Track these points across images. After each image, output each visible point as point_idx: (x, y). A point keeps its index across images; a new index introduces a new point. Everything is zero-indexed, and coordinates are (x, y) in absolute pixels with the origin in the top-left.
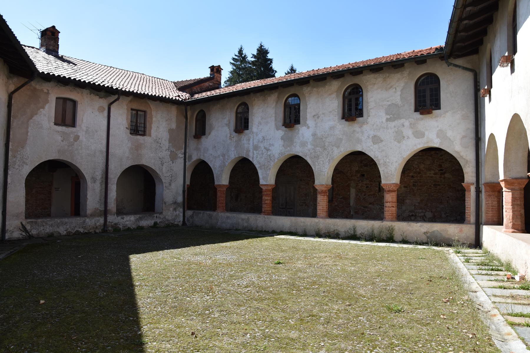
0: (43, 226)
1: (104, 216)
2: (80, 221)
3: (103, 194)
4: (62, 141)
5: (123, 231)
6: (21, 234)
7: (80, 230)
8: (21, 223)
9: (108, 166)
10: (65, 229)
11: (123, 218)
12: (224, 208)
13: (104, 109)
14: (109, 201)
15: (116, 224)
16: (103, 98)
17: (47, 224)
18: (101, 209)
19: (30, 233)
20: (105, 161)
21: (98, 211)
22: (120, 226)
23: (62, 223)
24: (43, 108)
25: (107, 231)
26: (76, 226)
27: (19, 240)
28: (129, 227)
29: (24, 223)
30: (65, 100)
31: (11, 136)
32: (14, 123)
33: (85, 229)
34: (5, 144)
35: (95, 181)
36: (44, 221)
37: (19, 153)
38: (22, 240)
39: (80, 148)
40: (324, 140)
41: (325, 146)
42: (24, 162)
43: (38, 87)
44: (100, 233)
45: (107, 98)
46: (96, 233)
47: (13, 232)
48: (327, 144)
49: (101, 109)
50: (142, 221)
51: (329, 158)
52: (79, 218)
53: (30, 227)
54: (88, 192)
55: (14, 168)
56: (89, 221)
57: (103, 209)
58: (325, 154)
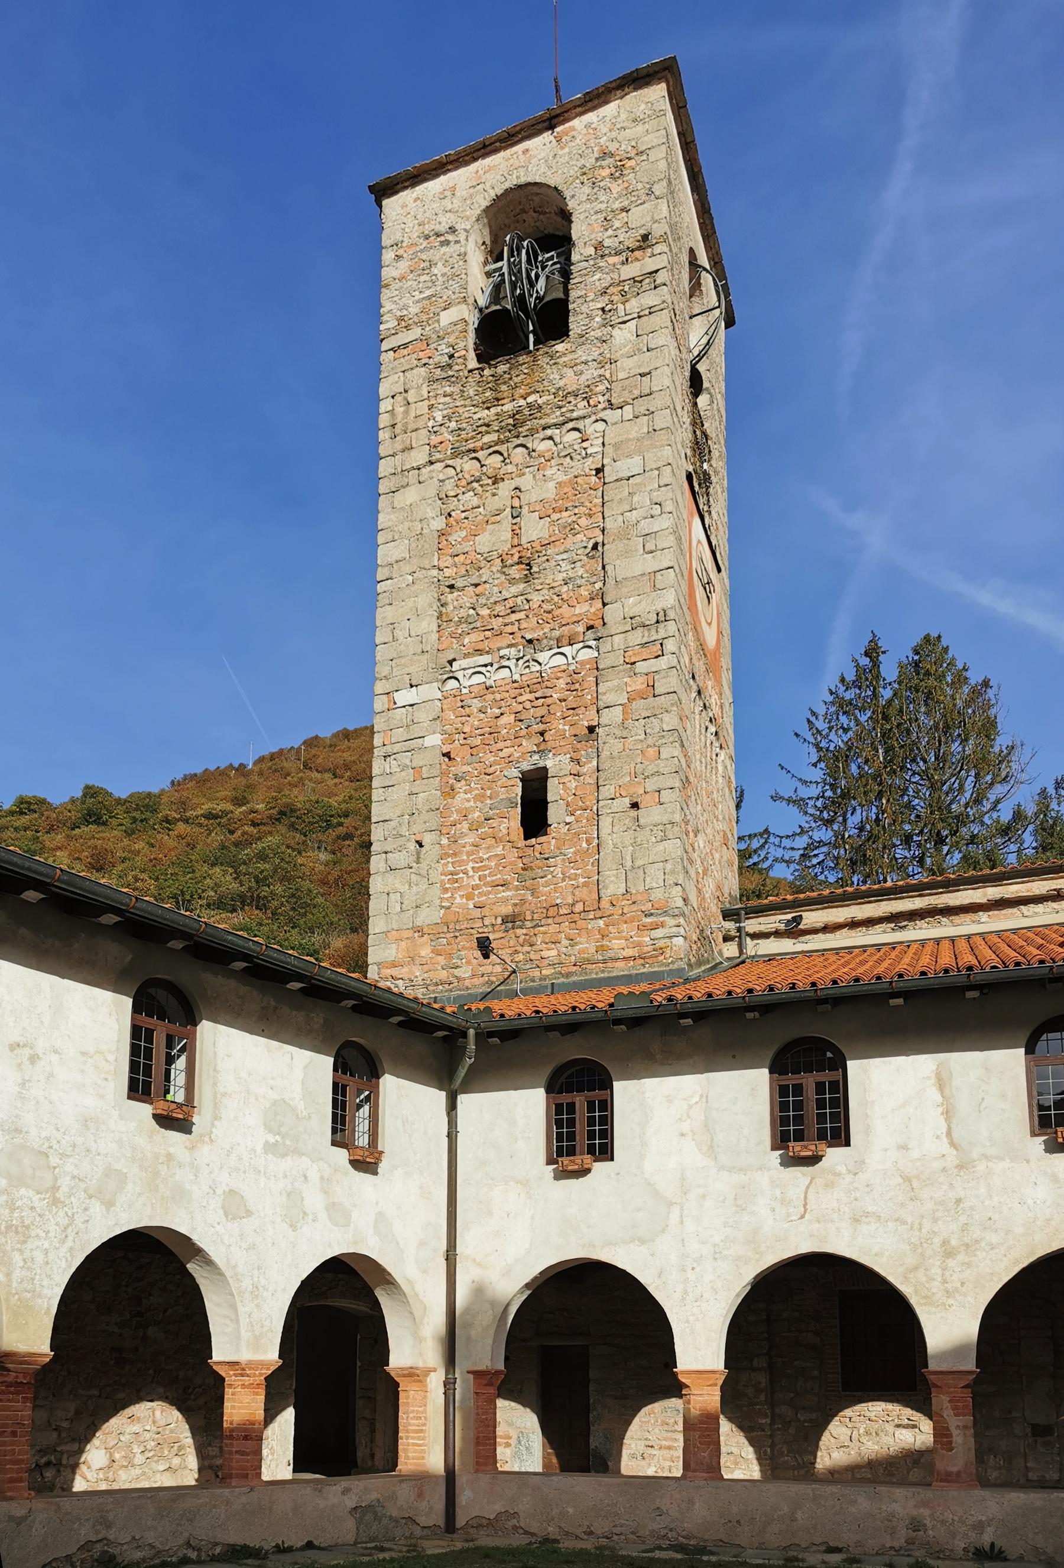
40: (54, 1161)
41: (55, 1188)
48: (65, 1183)
51: (69, 1243)
58: (57, 1224)
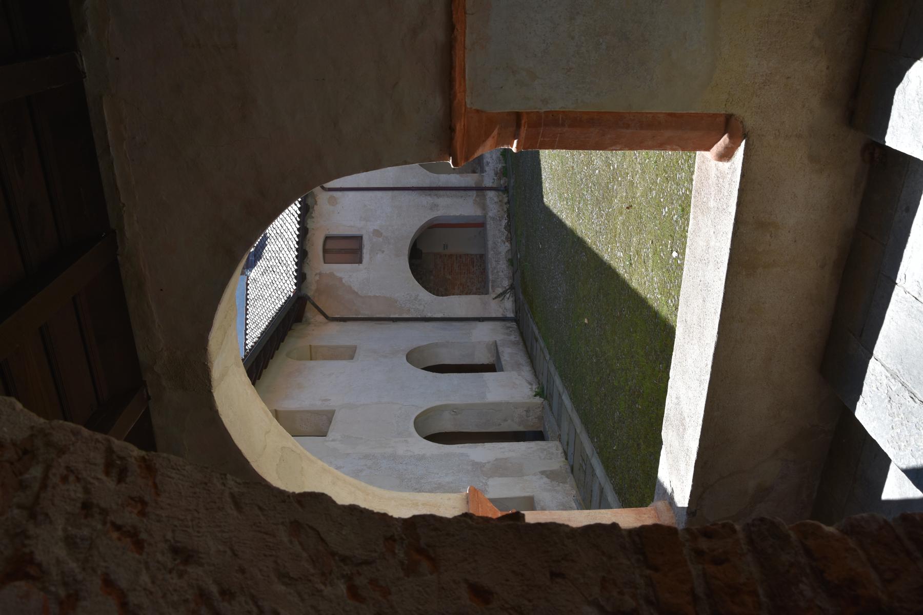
0: (498, 272)
1: (484, 191)
2: (492, 223)
3: (453, 192)
4: (383, 252)
5: (506, 163)
6: (508, 299)
8: (494, 299)
9: (413, 187)
10: (503, 244)
11: (488, 163)
13: (332, 197)
14: (463, 185)
15: (496, 174)
16: (316, 200)
17: (495, 268)
18: (475, 195)
19: (507, 288)
20: (406, 192)
21: (477, 199)
22: (499, 168)
23: (495, 248)
24: (341, 279)
25: (505, 187)
26: (499, 230)
27: (516, 301)
28: (501, 155)
30: (325, 251)
31: (383, 316)
32: (366, 313)
33: (502, 217)
34: (393, 321)
35: (435, 205)
37: (403, 305)
38: (515, 298)
44: (508, 196)
45: (315, 193)
46: (508, 202)
47: (505, 309)
49: (333, 202)
52: (488, 226)
54: (452, 215)
55: (423, 311)
57: (475, 192)
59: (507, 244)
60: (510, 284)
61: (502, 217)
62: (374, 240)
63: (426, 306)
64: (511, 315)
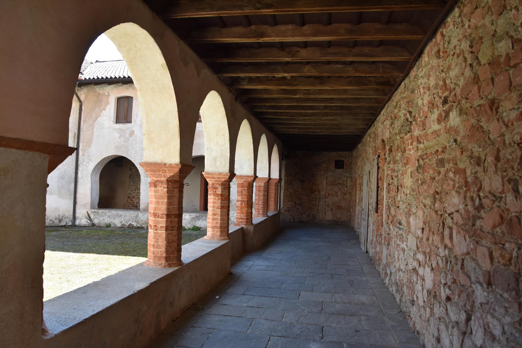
0: (103, 216)
2: (134, 215)
4: (120, 138)
7: (133, 224)
8: (87, 212)
10: (120, 221)
12: (261, 211)
17: (106, 214)
19: (93, 222)
23: (118, 216)
24: (105, 109)
26: (129, 220)
29: (89, 213)
33: (138, 223)
36: (104, 212)
37: (87, 151)
39: (134, 142)
42: (90, 160)
43: (101, 92)
50: (200, 222)
53: (93, 216)
55: (83, 165)
56: (142, 216)
59: (119, 225)
60: (96, 224)
61: (138, 223)
62: (127, 131)
63: (86, 167)
64: (77, 223)
